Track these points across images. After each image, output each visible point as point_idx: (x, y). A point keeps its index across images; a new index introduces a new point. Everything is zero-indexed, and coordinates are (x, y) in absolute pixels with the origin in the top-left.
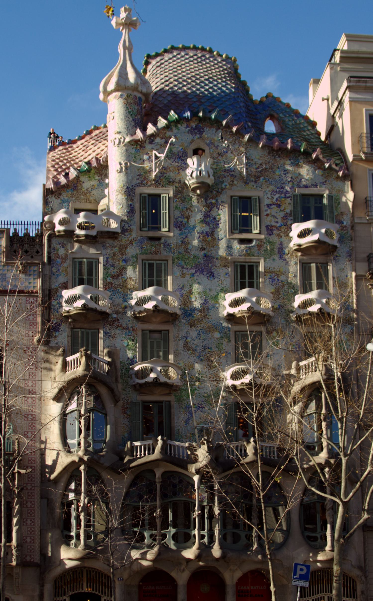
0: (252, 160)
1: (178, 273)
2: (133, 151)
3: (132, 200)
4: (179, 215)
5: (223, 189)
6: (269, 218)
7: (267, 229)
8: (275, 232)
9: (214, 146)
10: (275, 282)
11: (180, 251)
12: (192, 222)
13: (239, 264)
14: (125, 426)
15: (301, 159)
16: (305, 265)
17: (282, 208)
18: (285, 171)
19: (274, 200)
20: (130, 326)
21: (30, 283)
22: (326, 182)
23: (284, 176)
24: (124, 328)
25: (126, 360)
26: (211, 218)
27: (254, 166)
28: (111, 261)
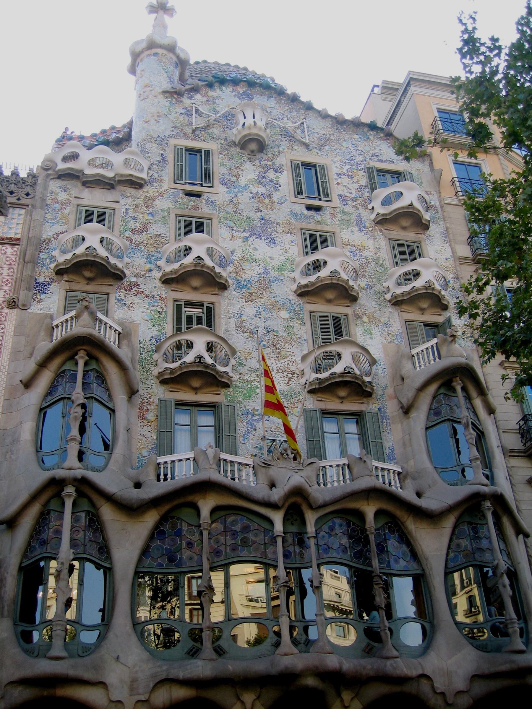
0: (314, 129)
2: (168, 104)
3: (164, 150)
4: (227, 173)
5: (280, 152)
6: (340, 187)
7: (340, 199)
9: (267, 112)
12: (243, 181)
13: (307, 232)
14: (144, 439)
15: (371, 135)
16: (393, 242)
17: (355, 179)
20: (155, 294)
21: (11, 228)
25: (148, 339)
26: (268, 180)
28: (131, 213)
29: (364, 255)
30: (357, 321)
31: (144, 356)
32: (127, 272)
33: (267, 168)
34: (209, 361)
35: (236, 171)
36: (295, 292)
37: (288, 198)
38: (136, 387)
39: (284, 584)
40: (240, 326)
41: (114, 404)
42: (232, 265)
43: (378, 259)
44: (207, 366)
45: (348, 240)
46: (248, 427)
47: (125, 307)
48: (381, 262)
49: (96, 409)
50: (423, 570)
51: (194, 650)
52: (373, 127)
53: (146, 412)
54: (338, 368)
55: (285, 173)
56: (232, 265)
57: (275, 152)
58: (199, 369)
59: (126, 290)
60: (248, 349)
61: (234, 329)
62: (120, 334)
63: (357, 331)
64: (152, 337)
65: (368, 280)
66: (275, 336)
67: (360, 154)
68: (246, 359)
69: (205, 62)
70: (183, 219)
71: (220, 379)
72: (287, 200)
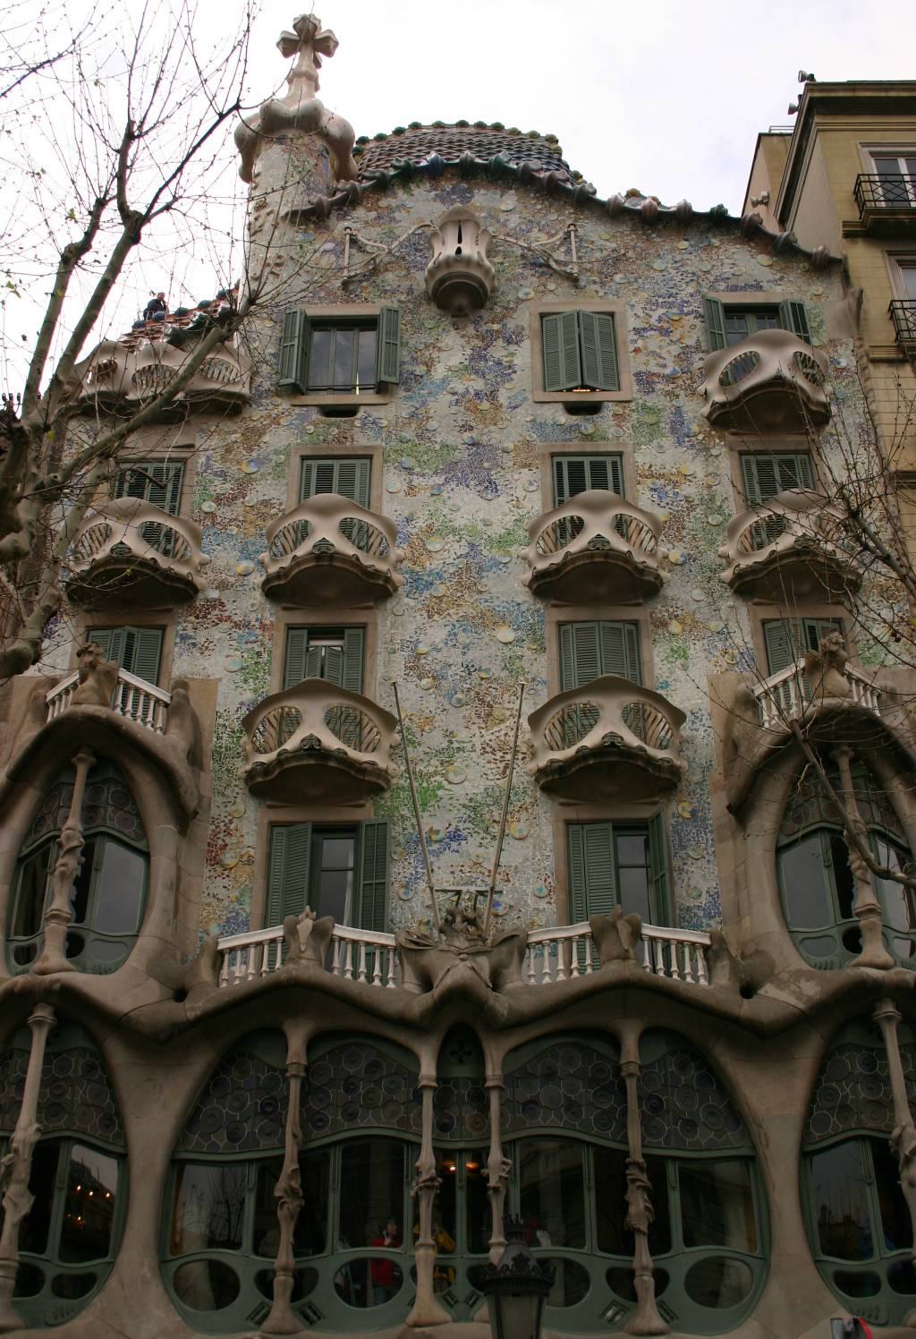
0: (593, 242)
1: (399, 486)
2: (300, 237)
6: (641, 358)
7: (639, 381)
8: (659, 386)
9: (498, 221)
10: (668, 500)
11: (403, 434)
12: (439, 371)
14: (215, 903)
15: (715, 236)
17: (675, 336)
18: (676, 262)
19: (653, 321)
20: (252, 617)
22: (781, 279)
23: (674, 272)
24: (237, 625)
26: (491, 363)
27: (598, 255)
29: (684, 493)
30: (656, 633)
31: (226, 740)
32: (199, 581)
33: (488, 339)
34: (331, 742)
35: (427, 353)
36: (529, 586)
37: (530, 396)
38: (192, 804)
39: (428, 1183)
40: (416, 666)
41: (148, 842)
42: (405, 546)
43: (712, 499)
44: (325, 754)
45: (651, 466)
46: (416, 867)
47: (193, 650)
48: (718, 503)
49: (111, 853)
50: (754, 1148)
51: (264, 1311)
52: (718, 219)
53: (221, 849)
54: (592, 740)
55: (526, 344)
56: (405, 546)
57: (509, 302)
58: (312, 762)
59: (197, 617)
60: (427, 711)
61: (402, 673)
62: (166, 705)
63: (655, 653)
64: (242, 703)
65: (688, 546)
66: (482, 679)
67: (688, 279)
68: (423, 730)
69: (416, 126)
70: (315, 463)
71: (361, 777)
72: (525, 399)
